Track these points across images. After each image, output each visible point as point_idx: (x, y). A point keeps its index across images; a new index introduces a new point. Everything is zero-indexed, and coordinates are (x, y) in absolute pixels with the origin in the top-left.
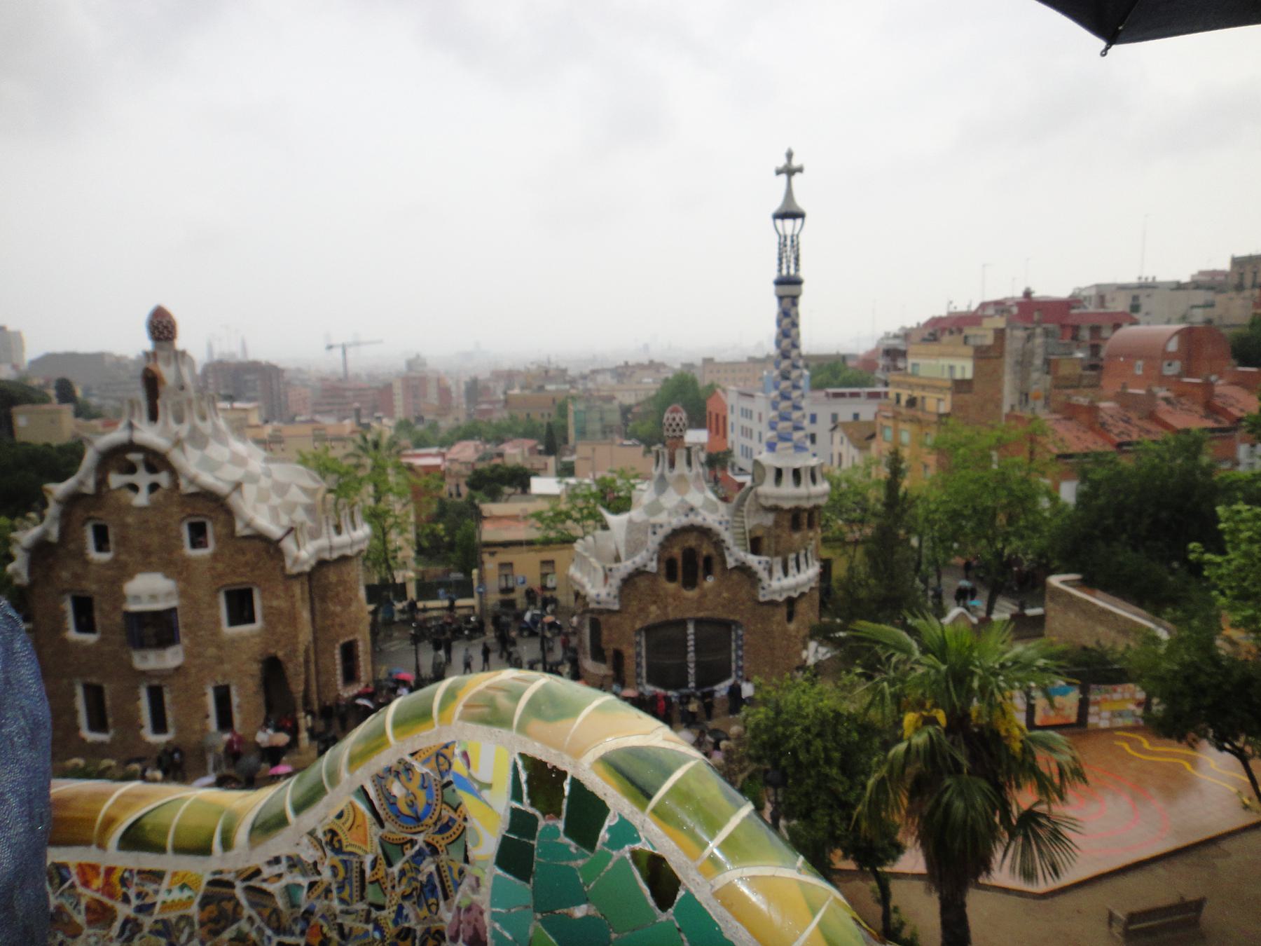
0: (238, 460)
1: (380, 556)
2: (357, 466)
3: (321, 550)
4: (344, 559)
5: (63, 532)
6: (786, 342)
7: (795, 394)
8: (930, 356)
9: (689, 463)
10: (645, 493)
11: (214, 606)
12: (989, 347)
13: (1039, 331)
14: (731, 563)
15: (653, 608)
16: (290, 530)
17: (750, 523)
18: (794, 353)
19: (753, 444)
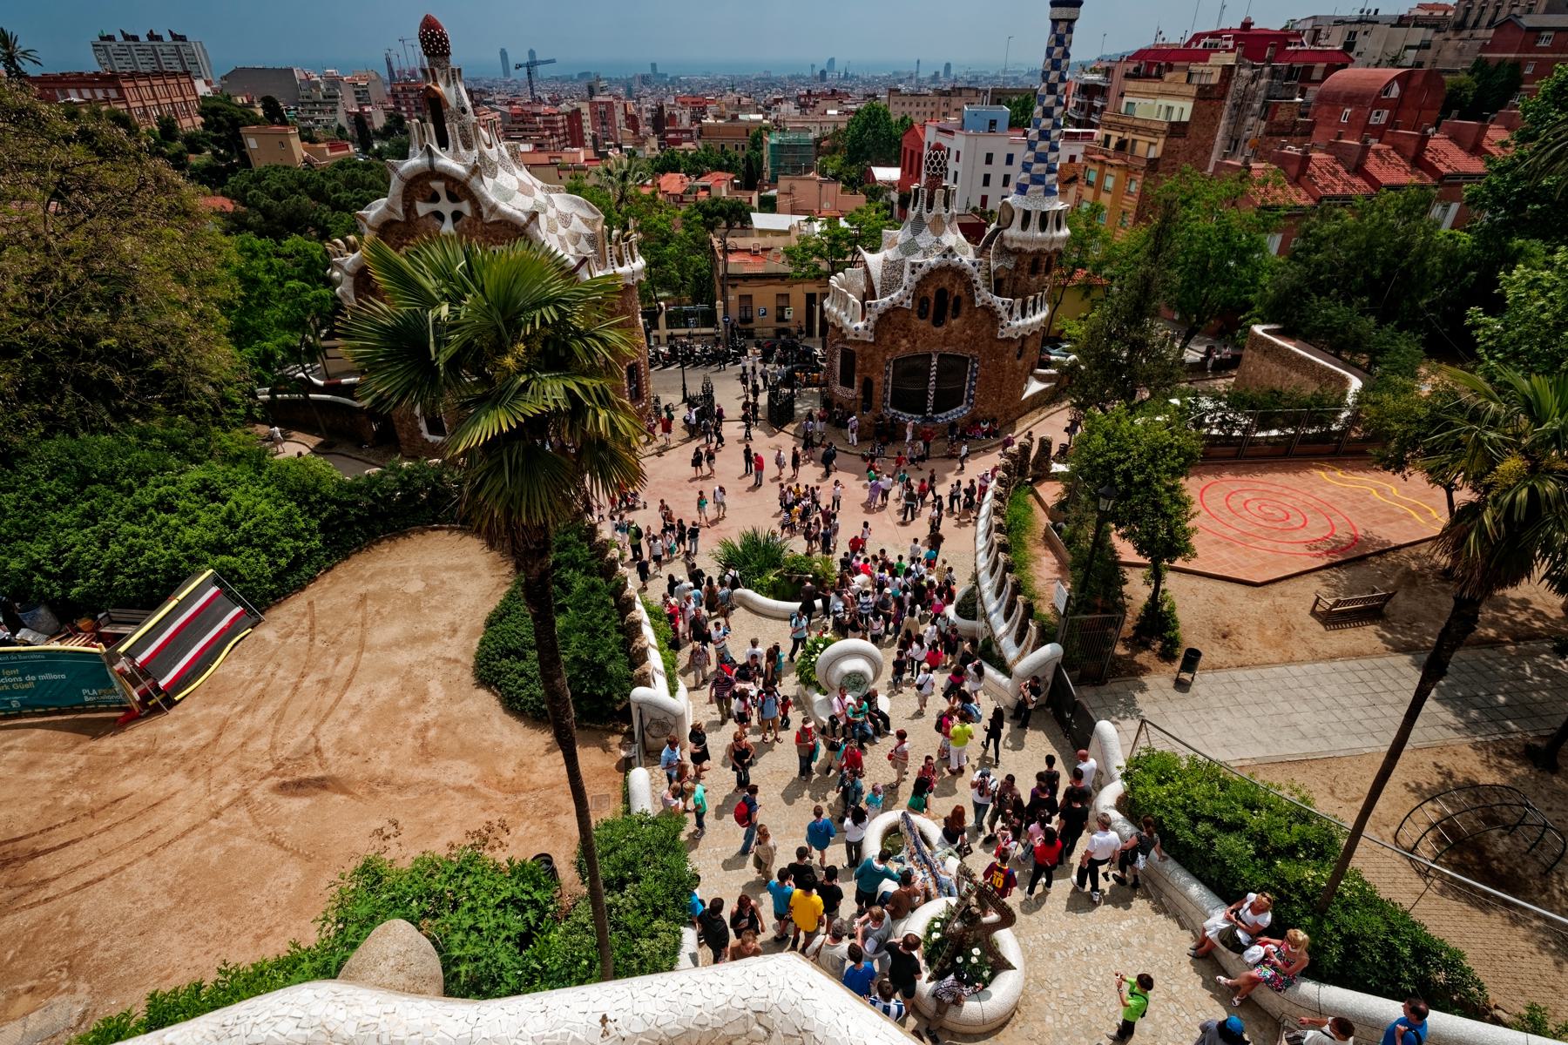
9: (946, 205)
14: (979, 302)
15: (904, 342)
17: (994, 265)
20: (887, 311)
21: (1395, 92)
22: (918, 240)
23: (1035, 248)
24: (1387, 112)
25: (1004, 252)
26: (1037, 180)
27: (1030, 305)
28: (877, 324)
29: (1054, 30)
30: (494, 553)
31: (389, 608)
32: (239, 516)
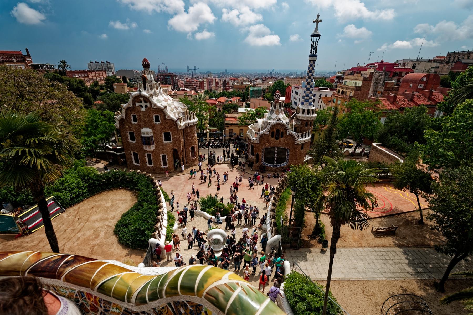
0: (166, 100)
1: (200, 126)
2: (195, 103)
3: (186, 124)
4: (191, 126)
5: (126, 116)
6: (310, 74)
7: (311, 89)
8: (350, 79)
9: (280, 107)
10: (267, 115)
11: (161, 136)
12: (368, 77)
13: (383, 73)
15: (267, 144)
16: (178, 119)
17: (294, 123)
18: (312, 77)
19: (297, 101)
20: (262, 135)
21: (425, 79)
22: (272, 116)
23: (306, 119)
24: (423, 85)
25: (298, 120)
26: (306, 101)
27: (304, 135)
28: (259, 138)
29: (310, 63)
30: (134, 197)
31: (99, 210)
32: (65, 181)
